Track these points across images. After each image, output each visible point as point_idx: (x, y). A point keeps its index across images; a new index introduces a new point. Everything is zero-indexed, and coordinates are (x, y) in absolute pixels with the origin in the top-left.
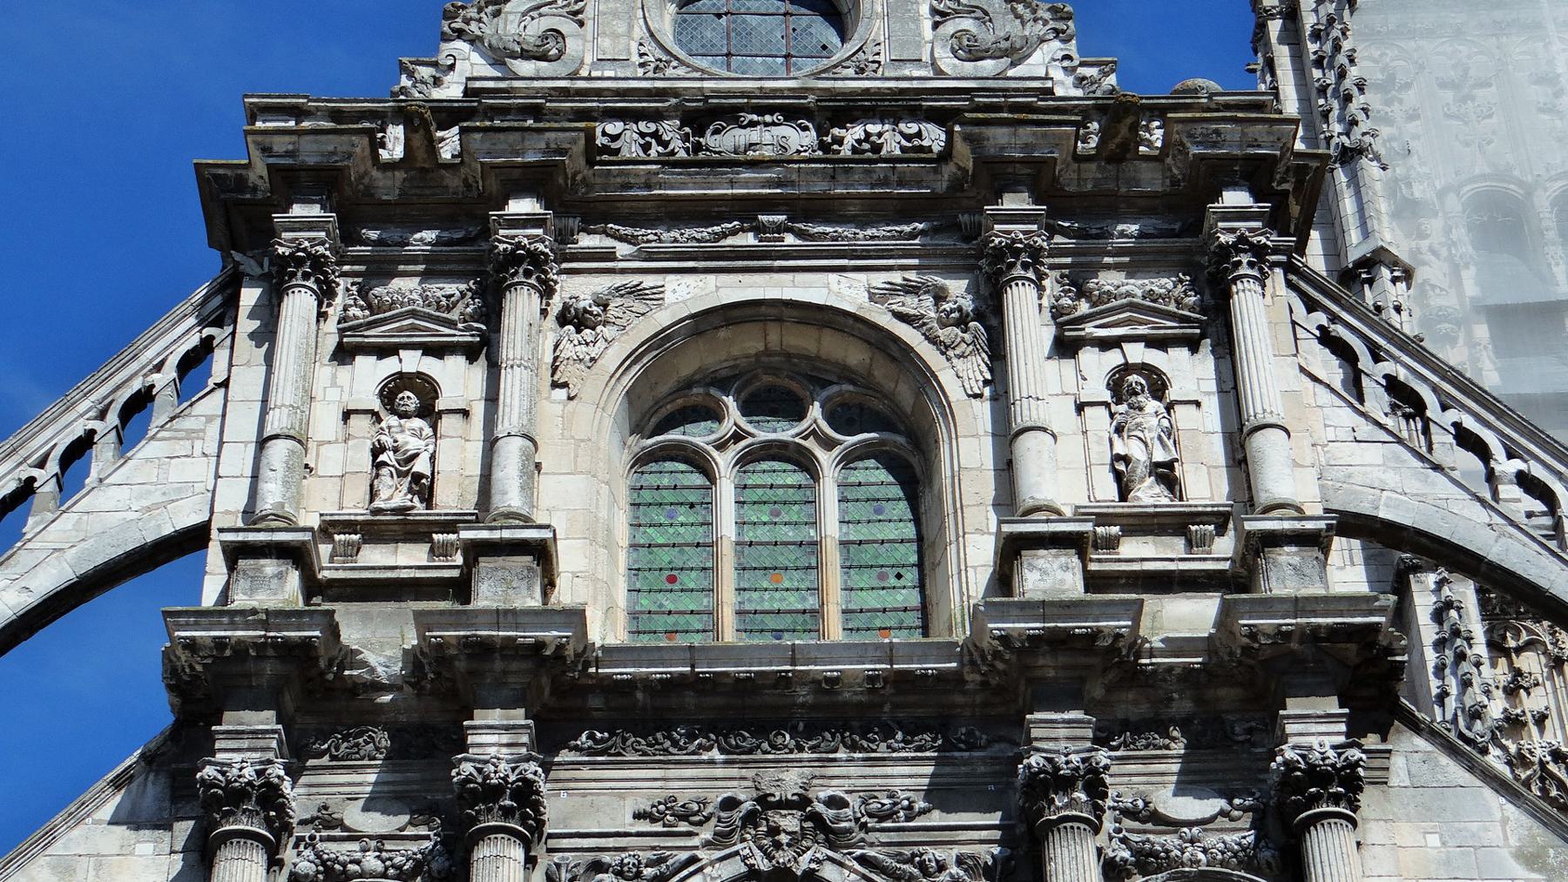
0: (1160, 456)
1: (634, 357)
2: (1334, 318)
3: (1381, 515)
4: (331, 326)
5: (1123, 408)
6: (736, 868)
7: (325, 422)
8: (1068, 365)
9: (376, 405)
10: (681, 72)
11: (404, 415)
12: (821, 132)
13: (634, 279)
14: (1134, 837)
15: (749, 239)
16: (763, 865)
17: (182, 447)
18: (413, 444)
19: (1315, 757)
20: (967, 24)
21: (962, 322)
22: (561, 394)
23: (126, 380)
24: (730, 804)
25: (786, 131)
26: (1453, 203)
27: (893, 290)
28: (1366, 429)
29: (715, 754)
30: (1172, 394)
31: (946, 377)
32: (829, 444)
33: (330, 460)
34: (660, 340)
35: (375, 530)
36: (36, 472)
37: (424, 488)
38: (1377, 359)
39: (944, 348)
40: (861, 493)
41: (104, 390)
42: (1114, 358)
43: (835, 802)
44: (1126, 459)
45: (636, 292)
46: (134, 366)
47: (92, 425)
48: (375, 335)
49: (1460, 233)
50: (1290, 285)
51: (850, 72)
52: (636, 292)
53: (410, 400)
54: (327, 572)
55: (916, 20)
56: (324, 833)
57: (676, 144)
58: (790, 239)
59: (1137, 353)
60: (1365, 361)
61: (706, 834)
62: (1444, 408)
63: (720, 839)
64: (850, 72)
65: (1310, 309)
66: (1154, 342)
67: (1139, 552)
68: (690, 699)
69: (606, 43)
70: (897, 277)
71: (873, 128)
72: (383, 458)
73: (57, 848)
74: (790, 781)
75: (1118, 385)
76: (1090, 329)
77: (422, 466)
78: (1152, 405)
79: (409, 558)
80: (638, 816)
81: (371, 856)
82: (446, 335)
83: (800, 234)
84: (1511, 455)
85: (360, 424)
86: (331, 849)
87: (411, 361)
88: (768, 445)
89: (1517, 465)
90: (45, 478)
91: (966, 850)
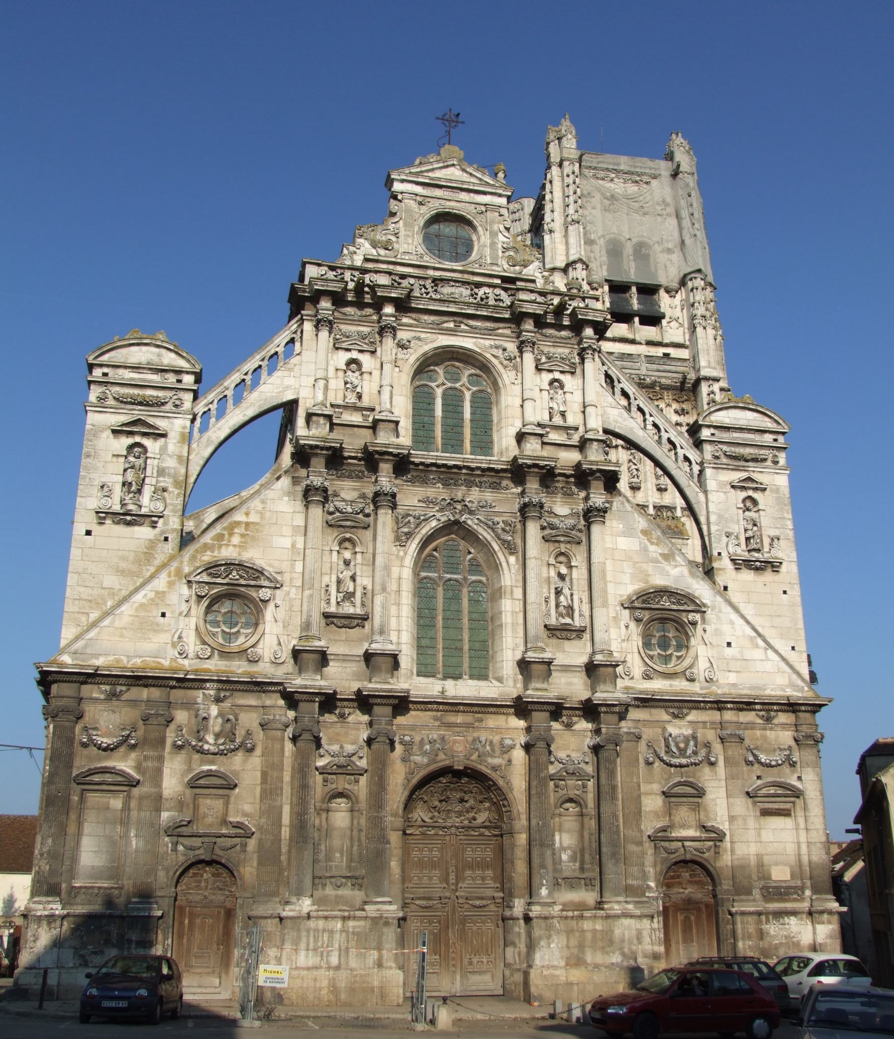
0: (562, 409)
1: (418, 359)
2: (609, 368)
3: (617, 430)
4: (331, 339)
5: (552, 392)
6: (443, 519)
7: (331, 373)
8: (538, 376)
9: (345, 368)
10: (428, 259)
11: (353, 372)
12: (472, 290)
13: (418, 334)
14: (548, 519)
15: (452, 325)
16: (452, 519)
17: (286, 373)
18: (356, 382)
19: (597, 505)
20: (512, 253)
21: (510, 360)
22: (397, 369)
23: (271, 349)
24: (444, 499)
25: (462, 289)
26: (602, 242)
27: (491, 347)
28: (614, 403)
29: (439, 485)
30: (566, 389)
31: (505, 376)
32: (469, 389)
33: (333, 384)
34: (424, 354)
35: (346, 407)
36: (245, 377)
37: (360, 397)
38: (619, 382)
39: (505, 367)
40: (476, 405)
41: (263, 353)
42: (550, 376)
43: (470, 501)
44: (551, 408)
45: (419, 339)
46: (272, 345)
47: (260, 363)
48: (344, 345)
49: (604, 252)
50: (599, 357)
51: (477, 266)
52: (419, 339)
53: (354, 366)
54: (335, 421)
55: (497, 250)
56: (336, 499)
57: (430, 290)
58: (463, 327)
59: (557, 375)
60: (616, 383)
61: (437, 508)
62: (636, 399)
63: (441, 510)
64: (477, 266)
65: (603, 365)
66: (562, 372)
67: (554, 437)
68: (434, 469)
69: (406, 246)
70: (492, 343)
71: (487, 290)
72: (348, 386)
73: (262, 496)
74: (459, 496)
75: (551, 383)
76: (546, 366)
77: (359, 390)
78: (560, 392)
79: (356, 418)
80: (419, 501)
81: (349, 507)
82: (365, 347)
83: (467, 325)
84: (651, 415)
85: (341, 374)
86: (338, 504)
87: (354, 355)
88: (451, 388)
89: (652, 419)
90: (248, 378)
91: (504, 519)
